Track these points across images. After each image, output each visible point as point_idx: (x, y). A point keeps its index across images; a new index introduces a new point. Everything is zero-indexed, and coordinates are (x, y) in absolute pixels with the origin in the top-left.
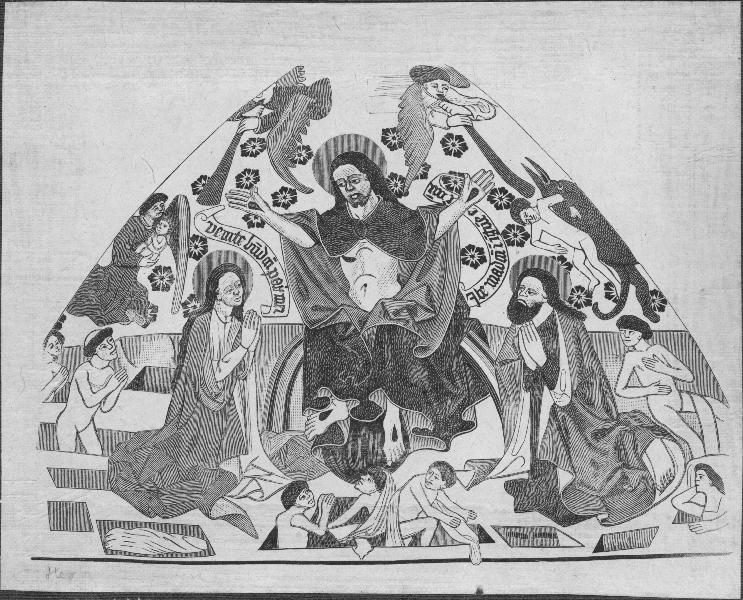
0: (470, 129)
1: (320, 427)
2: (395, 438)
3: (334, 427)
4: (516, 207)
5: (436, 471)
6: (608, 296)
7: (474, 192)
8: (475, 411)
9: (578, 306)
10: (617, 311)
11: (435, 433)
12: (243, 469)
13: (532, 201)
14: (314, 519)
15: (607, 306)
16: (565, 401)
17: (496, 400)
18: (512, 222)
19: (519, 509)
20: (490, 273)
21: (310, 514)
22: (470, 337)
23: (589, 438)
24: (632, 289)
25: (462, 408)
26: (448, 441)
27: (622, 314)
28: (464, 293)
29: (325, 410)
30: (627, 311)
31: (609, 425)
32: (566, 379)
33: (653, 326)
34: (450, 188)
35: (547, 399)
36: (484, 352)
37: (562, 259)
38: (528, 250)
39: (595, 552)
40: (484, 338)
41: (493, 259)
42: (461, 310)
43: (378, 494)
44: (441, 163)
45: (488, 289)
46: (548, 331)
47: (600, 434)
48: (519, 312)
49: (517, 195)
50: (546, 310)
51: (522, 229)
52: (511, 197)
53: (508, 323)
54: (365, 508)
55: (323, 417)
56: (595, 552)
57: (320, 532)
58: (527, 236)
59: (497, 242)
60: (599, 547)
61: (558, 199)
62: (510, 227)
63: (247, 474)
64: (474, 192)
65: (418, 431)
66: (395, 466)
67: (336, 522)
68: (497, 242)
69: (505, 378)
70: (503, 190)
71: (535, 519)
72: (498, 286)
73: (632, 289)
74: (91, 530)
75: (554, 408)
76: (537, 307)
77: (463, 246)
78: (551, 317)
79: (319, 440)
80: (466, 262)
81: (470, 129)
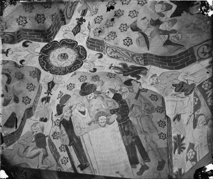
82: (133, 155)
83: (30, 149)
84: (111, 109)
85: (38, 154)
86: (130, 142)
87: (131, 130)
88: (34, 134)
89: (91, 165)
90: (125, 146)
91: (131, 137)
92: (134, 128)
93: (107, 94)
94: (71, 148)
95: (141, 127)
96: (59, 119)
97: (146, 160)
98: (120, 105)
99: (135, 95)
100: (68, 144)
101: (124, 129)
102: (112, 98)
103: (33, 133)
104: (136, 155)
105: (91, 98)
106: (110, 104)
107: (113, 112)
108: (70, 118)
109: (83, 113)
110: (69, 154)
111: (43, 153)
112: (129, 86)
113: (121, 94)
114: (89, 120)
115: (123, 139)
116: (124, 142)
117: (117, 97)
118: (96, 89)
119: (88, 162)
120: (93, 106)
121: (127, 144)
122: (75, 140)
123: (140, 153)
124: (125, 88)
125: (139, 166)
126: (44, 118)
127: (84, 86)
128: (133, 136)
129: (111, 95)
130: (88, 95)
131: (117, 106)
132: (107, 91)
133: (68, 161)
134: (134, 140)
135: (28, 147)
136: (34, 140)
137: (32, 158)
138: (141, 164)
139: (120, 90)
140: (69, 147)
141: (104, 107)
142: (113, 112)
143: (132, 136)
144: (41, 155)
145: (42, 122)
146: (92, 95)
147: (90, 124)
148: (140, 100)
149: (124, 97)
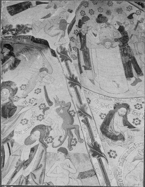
0: (45, 87)
4: (45, 109)
6: (59, 140)
7: (36, 104)
9: (48, 143)
10: (60, 145)
13: (51, 107)
15: (57, 143)
18: (42, 114)
20: (27, 127)
22: (8, 144)
24: (68, 137)
27: (61, 146)
28: (14, 132)
30: (63, 146)
32: (31, 168)
33: (69, 151)
34: (30, 102)
35: (21, 172)
36: (9, 149)
37: (50, 127)
38: (42, 123)
40: (12, 146)
41: (30, 124)
42: (12, 135)
44: (32, 95)
45: (23, 132)
46: (33, 150)
48: (28, 141)
49: (47, 105)
50: (37, 142)
51: (43, 116)
52: (45, 106)
53: (22, 143)
58: (43, 118)
59: (34, 119)
61: (59, 107)
62: (40, 115)
64: (36, 104)
68: (34, 119)
69: (11, 161)
70: (44, 104)
72: (26, 131)
73: (68, 137)
76: (35, 141)
77: (23, 118)
78: (37, 146)
80: (21, 123)
81: (45, 87)
82: (129, 70)
83: (54, 28)
84: (115, 38)
85: (58, 34)
86: (127, 61)
87: (129, 52)
88: (60, 19)
89: (93, 69)
90: (123, 63)
91: (129, 57)
92: (131, 52)
93: (115, 26)
94: (81, 53)
95: (137, 50)
96: (78, 30)
97: (139, 74)
98: (123, 35)
99: (134, 27)
100: (79, 48)
101: (124, 53)
102: (118, 30)
103: (60, 18)
104: (131, 71)
105: (103, 26)
106: (115, 34)
107: (116, 40)
108: (86, 35)
109: (95, 35)
110: (78, 55)
111: (61, 34)
112: (131, 19)
113: (124, 26)
114: (98, 41)
115: (122, 59)
116: (122, 61)
117: (121, 29)
118: (107, 21)
119: (91, 67)
120: (103, 33)
121: (124, 63)
122: (85, 49)
123: (135, 69)
124: (128, 21)
125: (133, 79)
126: (71, 10)
127: (100, 16)
128: (130, 57)
129: (117, 27)
130: (102, 24)
131: (120, 36)
132: (115, 23)
133: (76, 59)
134: (130, 60)
135: (53, 26)
136: (59, 23)
137: (53, 36)
138: (135, 78)
139: (124, 23)
140: (80, 50)
141: (111, 36)
142: (116, 40)
143: (129, 56)
144: (61, 34)
145: (68, 12)
146: (103, 25)
147: (98, 44)
148: (138, 31)
149: (126, 29)
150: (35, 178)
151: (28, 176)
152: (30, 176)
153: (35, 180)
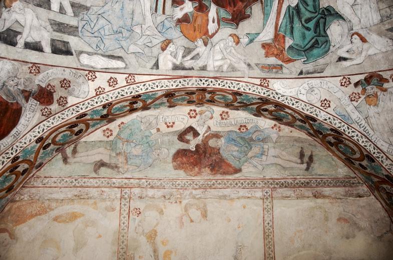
1: (179, 13)
2: (213, 22)
3: (186, 15)
5: (231, 39)
8: (251, 9)
11: (232, 20)
12: (143, 31)
14: (175, 57)
16: (293, 5)
17: (262, 3)
19: (267, 55)
21: (173, 54)
23: (303, 22)
25: (246, 7)
26: (238, 25)
29: (182, 6)
31: (313, 15)
39: (299, 75)
43: (204, 48)
47: (308, 20)
54: (198, 54)
55: (182, 9)
56: (299, 75)
57: (178, 63)
60: (301, 73)
63: (144, 34)
65: (224, 20)
66: (214, 35)
67: (185, 59)
71: (273, 60)
74: (75, 51)
75: (289, 7)
79: (179, 21)
150: (308, 5)
151: (297, 5)
152: (301, 6)
153: (309, 8)
